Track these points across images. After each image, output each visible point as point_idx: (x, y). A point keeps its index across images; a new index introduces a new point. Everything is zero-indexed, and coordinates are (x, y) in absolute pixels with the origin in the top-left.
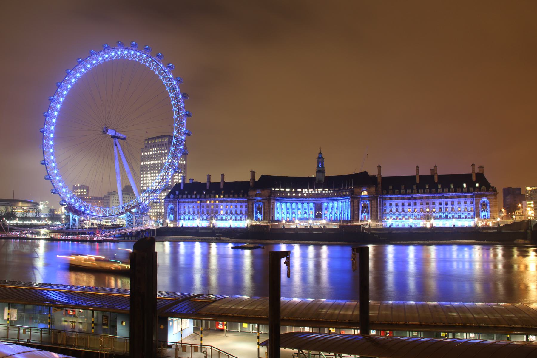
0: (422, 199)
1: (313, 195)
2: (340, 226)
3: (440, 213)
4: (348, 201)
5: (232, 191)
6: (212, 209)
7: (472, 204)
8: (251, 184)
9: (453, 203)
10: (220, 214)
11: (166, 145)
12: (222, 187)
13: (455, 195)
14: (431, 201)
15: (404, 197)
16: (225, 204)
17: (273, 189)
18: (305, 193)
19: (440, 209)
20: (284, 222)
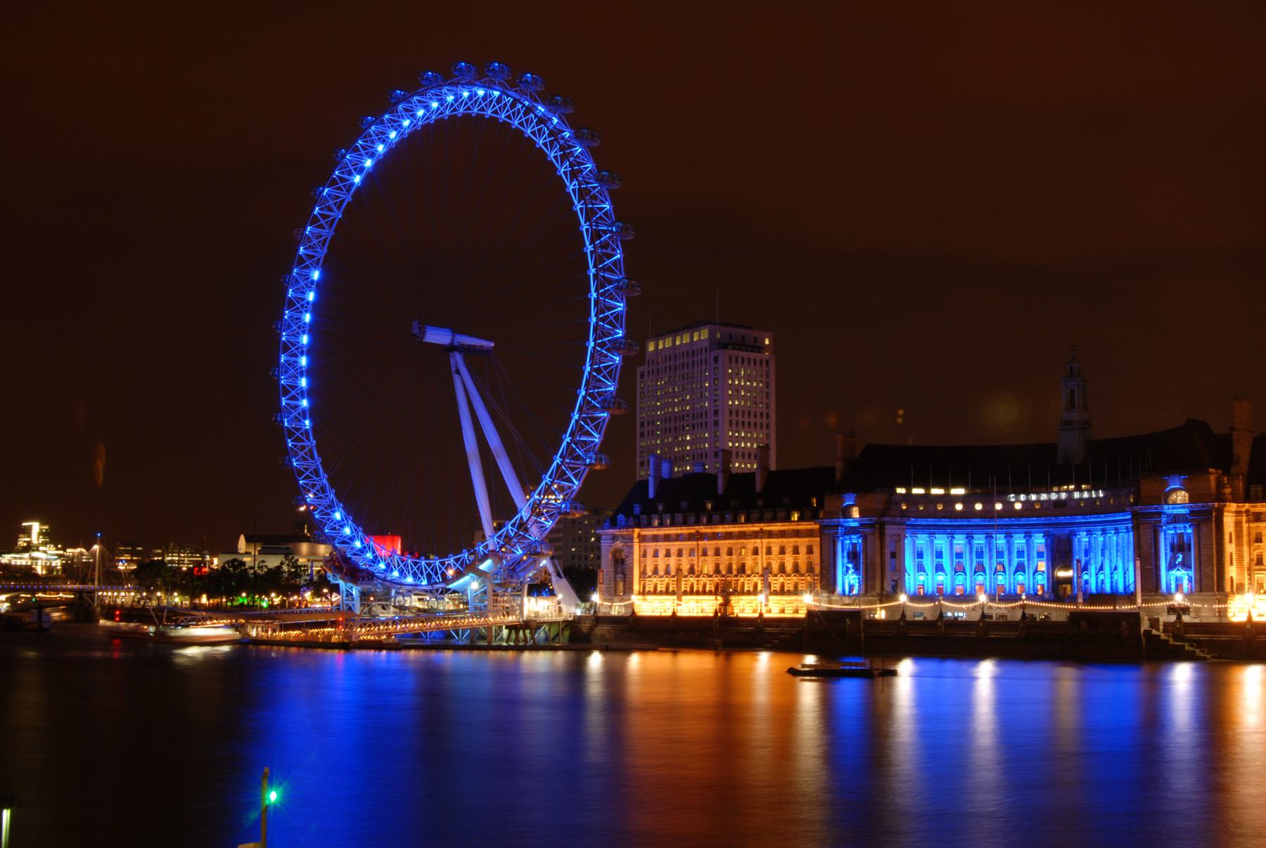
1: (1042, 506)
4: (1127, 528)
8: (838, 475)
11: (704, 353)
12: (758, 487)
16: (765, 541)
17: (901, 491)
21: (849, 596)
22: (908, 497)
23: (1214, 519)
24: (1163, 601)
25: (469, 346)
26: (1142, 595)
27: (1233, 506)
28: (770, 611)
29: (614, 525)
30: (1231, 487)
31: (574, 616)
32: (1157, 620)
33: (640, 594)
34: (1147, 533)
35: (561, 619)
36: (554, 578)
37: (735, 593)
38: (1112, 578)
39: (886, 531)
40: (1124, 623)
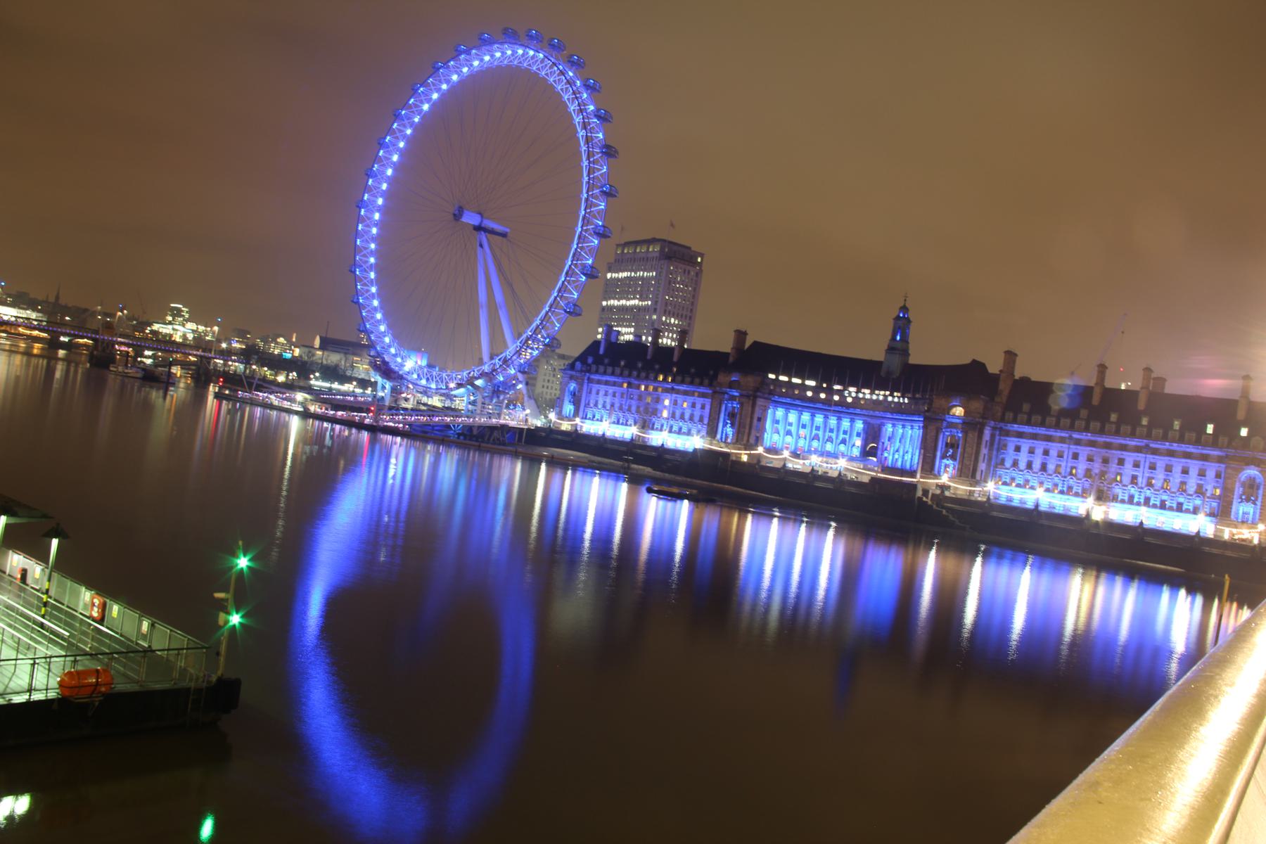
0: (1094, 446)
2: (874, 480)
3: (1133, 489)
4: (919, 427)
5: (693, 370)
6: (648, 404)
7: (1220, 478)
8: (731, 359)
9: (1169, 469)
10: (661, 416)
12: (675, 358)
13: (1178, 449)
14: (1118, 453)
15: (1051, 436)
16: (674, 395)
17: (772, 376)
18: (850, 395)
19: (1134, 478)
20: (786, 454)
24: (934, 479)
27: (992, 423)
35: (526, 427)
38: (903, 458)
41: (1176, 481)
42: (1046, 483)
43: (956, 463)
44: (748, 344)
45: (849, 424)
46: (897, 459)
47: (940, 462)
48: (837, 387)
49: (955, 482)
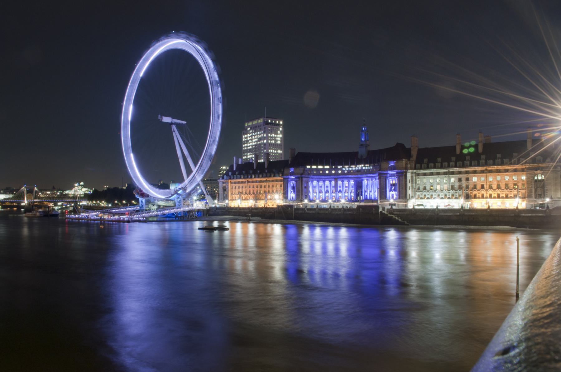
3: (483, 191)
8: (289, 162)
12: (266, 166)
16: (268, 183)
17: (308, 167)
21: (292, 200)
22: (311, 169)
23: (404, 175)
24: (387, 202)
25: (178, 123)
26: (380, 200)
27: (411, 170)
28: (269, 205)
29: (223, 178)
30: (410, 165)
31: (210, 207)
32: (385, 208)
33: (231, 200)
34: (383, 180)
35: (206, 208)
36: (206, 195)
37: (259, 199)
38: (374, 194)
39: (303, 180)
40: (373, 209)
41: (503, 184)
42: (440, 195)
43: (397, 193)
44: (296, 154)
45: (347, 183)
46: (371, 195)
47: (389, 194)
48: (339, 167)
49: (396, 202)
